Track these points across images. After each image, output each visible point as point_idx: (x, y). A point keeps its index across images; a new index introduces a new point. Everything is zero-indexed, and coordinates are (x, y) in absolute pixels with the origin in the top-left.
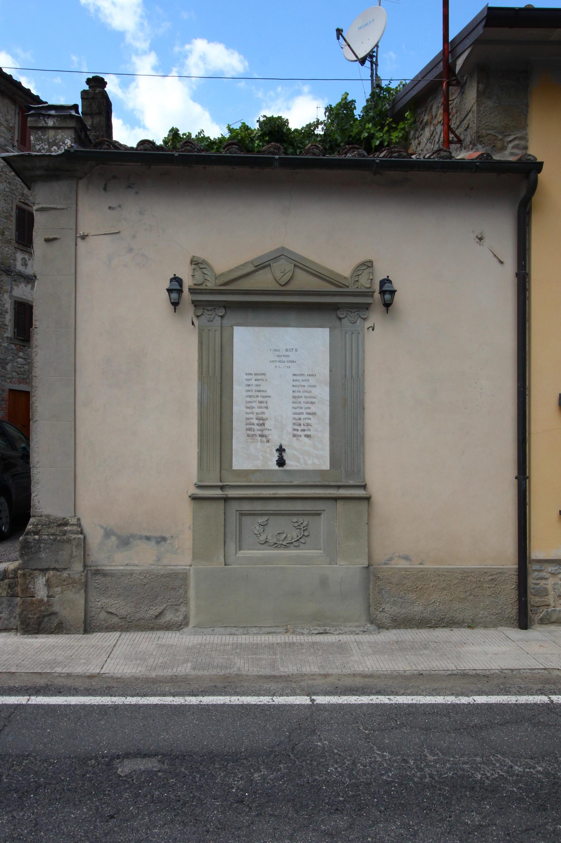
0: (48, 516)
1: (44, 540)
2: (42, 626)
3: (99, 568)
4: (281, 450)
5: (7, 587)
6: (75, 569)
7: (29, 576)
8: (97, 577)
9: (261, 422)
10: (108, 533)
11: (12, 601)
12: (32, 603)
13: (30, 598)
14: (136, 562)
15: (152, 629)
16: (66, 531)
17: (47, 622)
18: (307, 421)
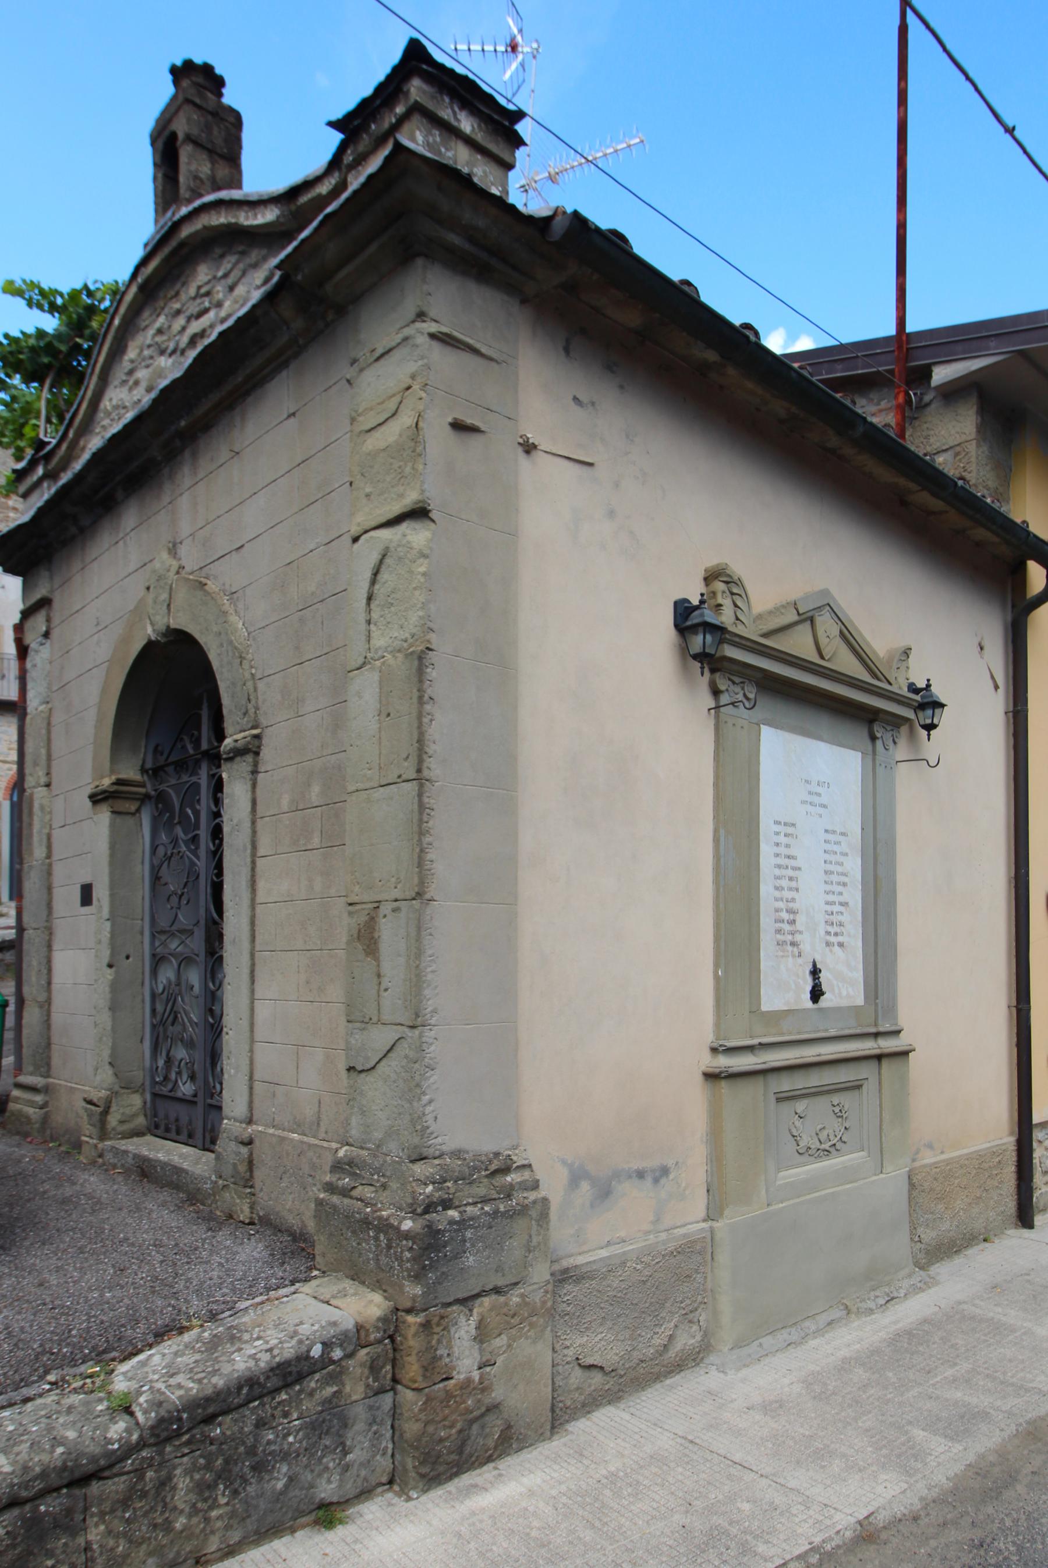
0: (457, 1154)
1: (472, 1219)
2: (468, 1450)
3: (565, 1263)
4: (815, 972)
5: (366, 1371)
6: (535, 1280)
7: (438, 1325)
8: (568, 1287)
9: (792, 917)
10: (576, 1177)
11: (378, 1408)
12: (449, 1395)
13: (441, 1385)
14: (622, 1234)
16: (512, 1186)
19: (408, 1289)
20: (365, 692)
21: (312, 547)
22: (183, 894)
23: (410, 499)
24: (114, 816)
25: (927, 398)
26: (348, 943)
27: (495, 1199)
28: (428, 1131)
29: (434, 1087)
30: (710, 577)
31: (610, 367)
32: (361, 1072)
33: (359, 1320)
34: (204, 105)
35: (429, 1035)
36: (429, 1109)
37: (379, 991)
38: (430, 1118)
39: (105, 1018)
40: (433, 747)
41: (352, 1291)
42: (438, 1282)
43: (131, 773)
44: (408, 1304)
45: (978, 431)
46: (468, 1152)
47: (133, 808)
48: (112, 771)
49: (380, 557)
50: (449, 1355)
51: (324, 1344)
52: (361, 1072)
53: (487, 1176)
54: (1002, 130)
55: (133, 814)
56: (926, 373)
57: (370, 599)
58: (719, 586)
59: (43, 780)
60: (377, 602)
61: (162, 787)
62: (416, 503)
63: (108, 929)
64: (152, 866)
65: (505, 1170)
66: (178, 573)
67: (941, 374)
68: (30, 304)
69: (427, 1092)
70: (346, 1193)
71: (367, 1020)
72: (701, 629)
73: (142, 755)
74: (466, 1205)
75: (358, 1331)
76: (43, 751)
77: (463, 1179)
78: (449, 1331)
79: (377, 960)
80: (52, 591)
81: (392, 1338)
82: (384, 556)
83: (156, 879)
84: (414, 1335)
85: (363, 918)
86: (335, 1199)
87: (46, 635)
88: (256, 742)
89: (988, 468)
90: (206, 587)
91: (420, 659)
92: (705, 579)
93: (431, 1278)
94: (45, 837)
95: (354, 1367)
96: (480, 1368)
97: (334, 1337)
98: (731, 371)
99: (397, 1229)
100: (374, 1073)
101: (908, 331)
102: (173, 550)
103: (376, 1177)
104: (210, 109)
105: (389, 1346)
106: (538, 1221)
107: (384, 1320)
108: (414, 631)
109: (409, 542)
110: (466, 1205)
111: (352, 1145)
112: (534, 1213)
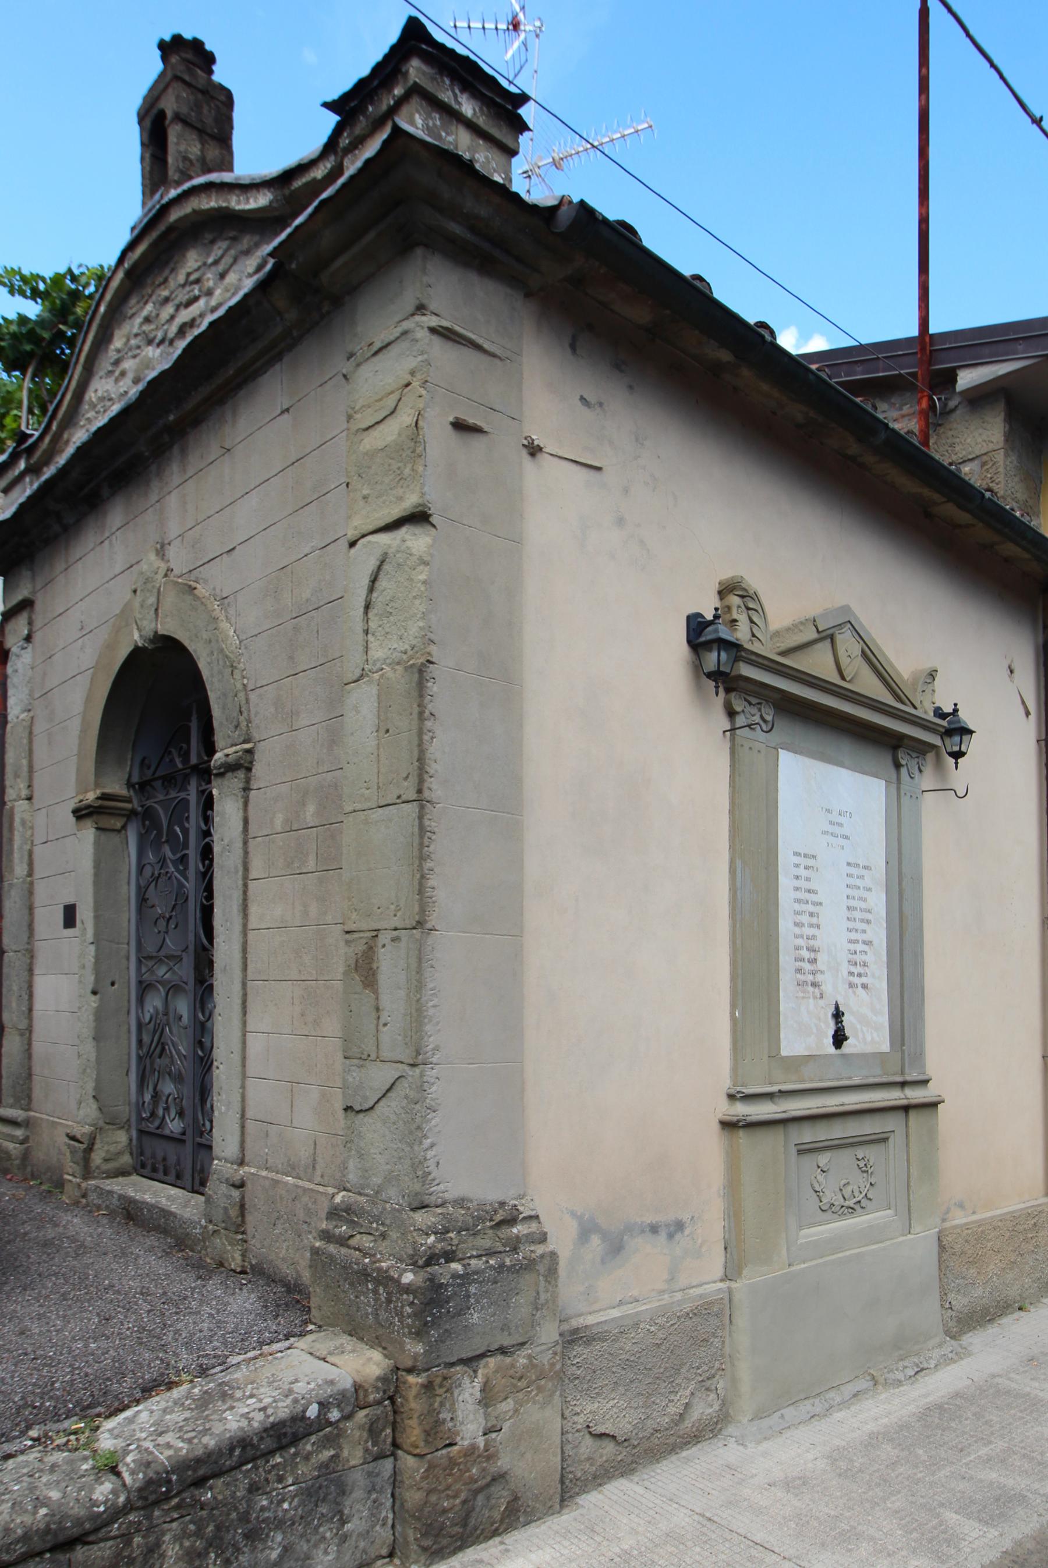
0: (460, 1202)
1: (476, 1273)
2: (472, 1522)
3: (575, 1323)
4: (838, 1015)
5: (365, 1435)
6: (543, 1340)
7: (441, 1386)
8: (578, 1349)
9: (813, 955)
10: (586, 1231)
11: (378, 1475)
12: (452, 1462)
13: (444, 1451)
14: (635, 1293)
15: (673, 1449)
17: (483, 1506)
18: (864, 957)
19: (408, 1347)
20: (363, 702)
21: (307, 551)
22: (171, 917)
23: (410, 502)
24: (98, 832)
25: (952, 404)
26: (345, 973)
27: (500, 1252)
28: (430, 1177)
29: (436, 1130)
30: (725, 590)
31: (618, 366)
32: (359, 1112)
33: (357, 1380)
34: (194, 83)
35: (430, 1074)
36: (430, 1154)
37: (377, 1026)
38: (431, 1163)
39: (89, 1048)
40: (434, 766)
41: (349, 1348)
42: (441, 1340)
43: (116, 787)
44: (409, 1363)
45: (1006, 441)
46: (471, 1201)
47: (119, 825)
48: (97, 785)
49: (378, 563)
50: (452, 1419)
51: (320, 1403)
52: (359, 1112)
53: (492, 1227)
54: (1029, 120)
55: (119, 831)
56: (950, 377)
57: (367, 607)
58: (734, 600)
59: (24, 793)
60: (375, 611)
61: (149, 803)
62: (416, 507)
63: (93, 953)
64: (139, 887)
65: (511, 1221)
66: (166, 575)
67: (966, 379)
68: (12, 292)
69: (429, 1135)
70: (343, 1241)
71: (365, 1057)
72: (715, 646)
73: (128, 769)
74: (470, 1258)
75: (356, 1391)
76: (25, 762)
77: (467, 1230)
78: (452, 1394)
79: (376, 992)
80: (34, 592)
81: (391, 1399)
82: (382, 562)
83: (142, 901)
84: (416, 1397)
85: (361, 948)
86: (332, 1248)
87: (28, 639)
88: (248, 757)
89: (1016, 479)
90: (196, 592)
91: (421, 673)
92: (720, 593)
93: (433, 1336)
94: (26, 854)
95: (352, 1430)
96: (485, 1434)
97: (331, 1396)
98: (746, 372)
99: (397, 1282)
100: (372, 1113)
101: (931, 332)
102: (161, 551)
103: (374, 1225)
104: (200, 86)
105: (389, 1408)
106: (545, 1276)
107: (384, 1379)
108: (414, 642)
109: (408, 548)
110: (470, 1258)
111: (349, 1191)
112: (541, 1268)
